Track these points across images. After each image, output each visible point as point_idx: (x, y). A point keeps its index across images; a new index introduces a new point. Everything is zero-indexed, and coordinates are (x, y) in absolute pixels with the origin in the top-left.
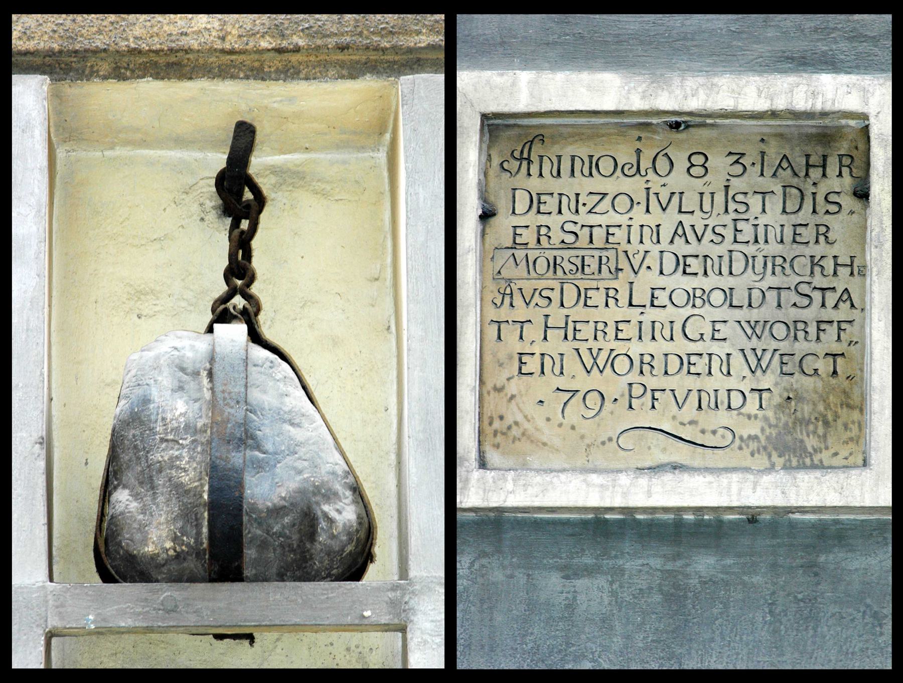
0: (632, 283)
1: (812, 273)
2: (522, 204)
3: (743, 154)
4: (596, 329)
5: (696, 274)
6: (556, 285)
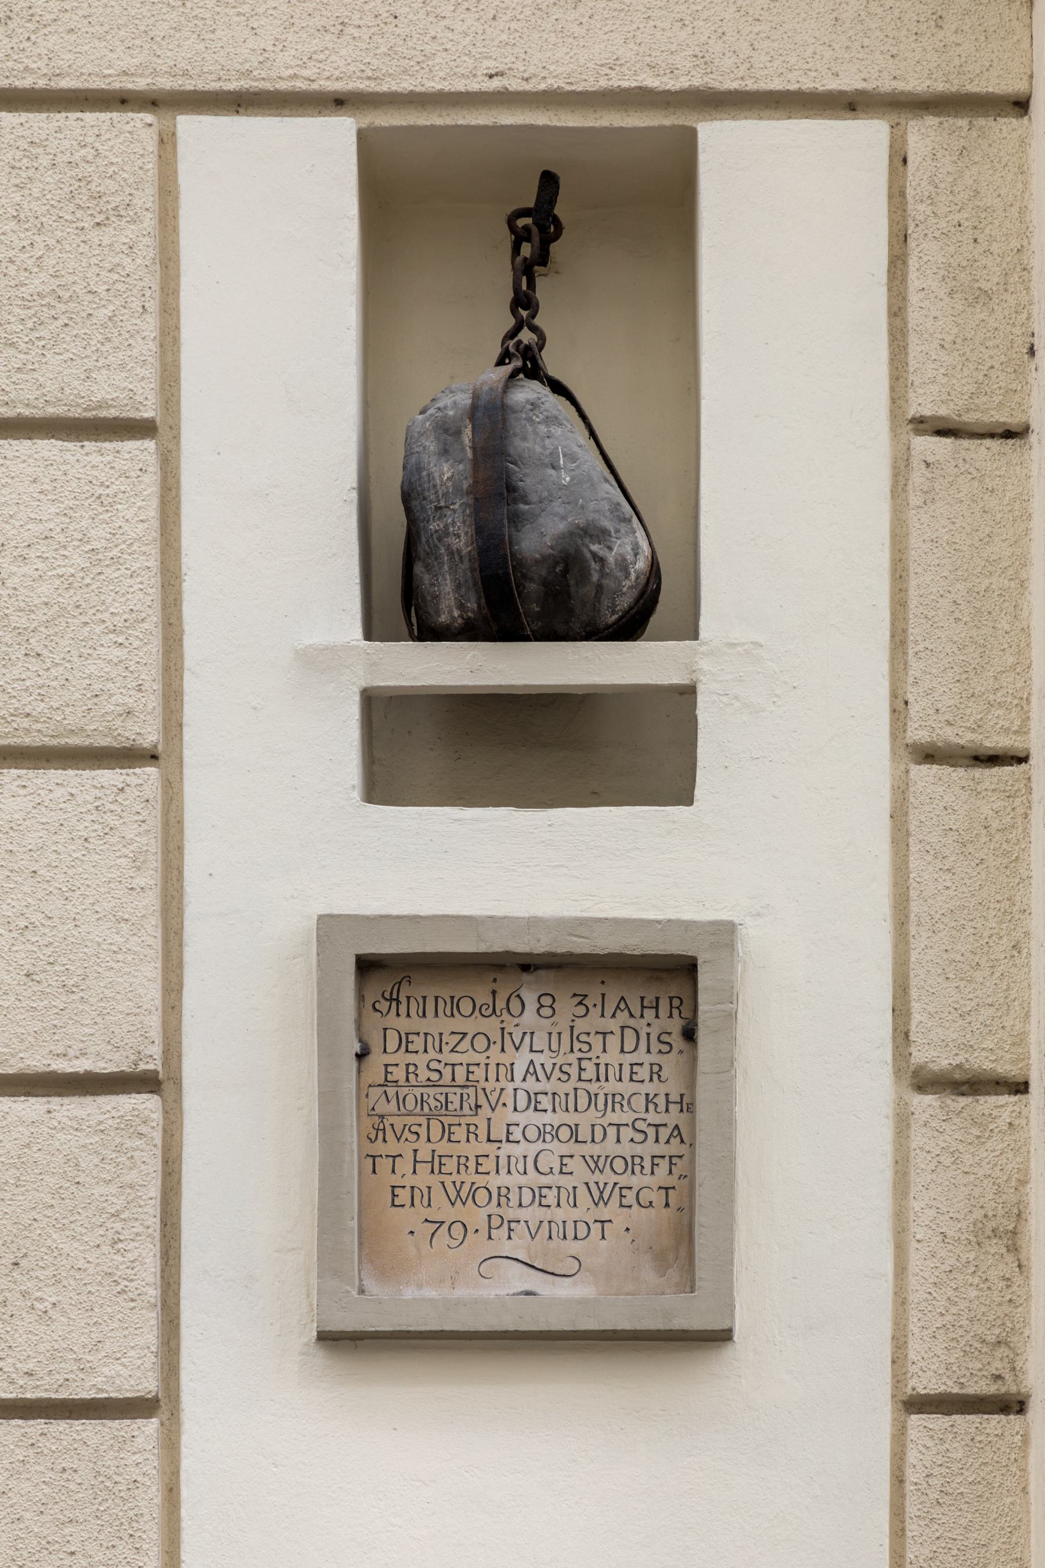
0: (489, 1119)
1: (647, 1110)
2: (392, 1044)
3: (586, 996)
4: (459, 1164)
5: (545, 1111)
6: (423, 1120)
